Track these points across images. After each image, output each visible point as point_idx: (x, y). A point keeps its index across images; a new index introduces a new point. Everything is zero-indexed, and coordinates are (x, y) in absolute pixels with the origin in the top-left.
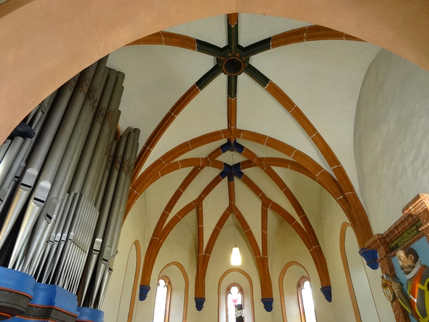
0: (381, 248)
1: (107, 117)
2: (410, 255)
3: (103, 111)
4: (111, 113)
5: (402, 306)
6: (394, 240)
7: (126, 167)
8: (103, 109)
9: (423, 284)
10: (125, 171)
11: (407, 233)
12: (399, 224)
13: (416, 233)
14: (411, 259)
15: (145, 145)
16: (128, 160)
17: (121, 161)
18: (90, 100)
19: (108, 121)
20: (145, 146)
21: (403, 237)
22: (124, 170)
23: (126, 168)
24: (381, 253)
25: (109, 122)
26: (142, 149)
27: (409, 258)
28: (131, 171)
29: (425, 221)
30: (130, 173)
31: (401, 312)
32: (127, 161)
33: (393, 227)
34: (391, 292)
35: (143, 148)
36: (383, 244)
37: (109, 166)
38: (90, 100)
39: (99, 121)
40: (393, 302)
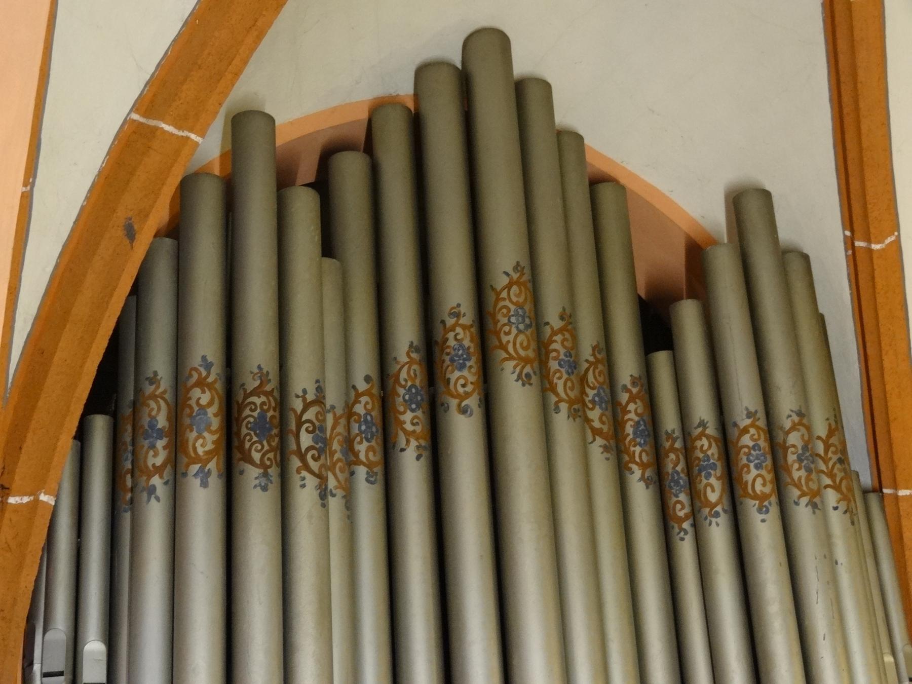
1: (493, 341)
3: (451, 335)
4: (501, 304)
7: (752, 465)
8: (450, 322)
10: (755, 497)
15: (844, 229)
16: (748, 422)
17: (714, 451)
18: (252, 462)
19: (505, 355)
20: (848, 233)
22: (747, 494)
23: (754, 472)
25: (511, 358)
26: (847, 256)
28: (800, 460)
30: (796, 475)
32: (745, 431)
35: (846, 251)
37: (679, 506)
38: (252, 462)
39: (453, 403)
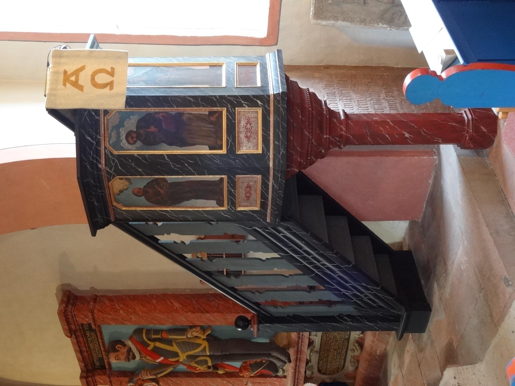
0: (97, 379)
2: (116, 347)
5: (165, 376)
6: (93, 360)
9: (149, 345)
11: (91, 343)
12: (79, 347)
13: (94, 333)
14: (120, 347)
21: (93, 349)
24: (102, 382)
27: (119, 349)
29: (87, 319)
31: (170, 378)
33: (79, 355)
34: (150, 383)
36: (94, 375)
40: (159, 384)
